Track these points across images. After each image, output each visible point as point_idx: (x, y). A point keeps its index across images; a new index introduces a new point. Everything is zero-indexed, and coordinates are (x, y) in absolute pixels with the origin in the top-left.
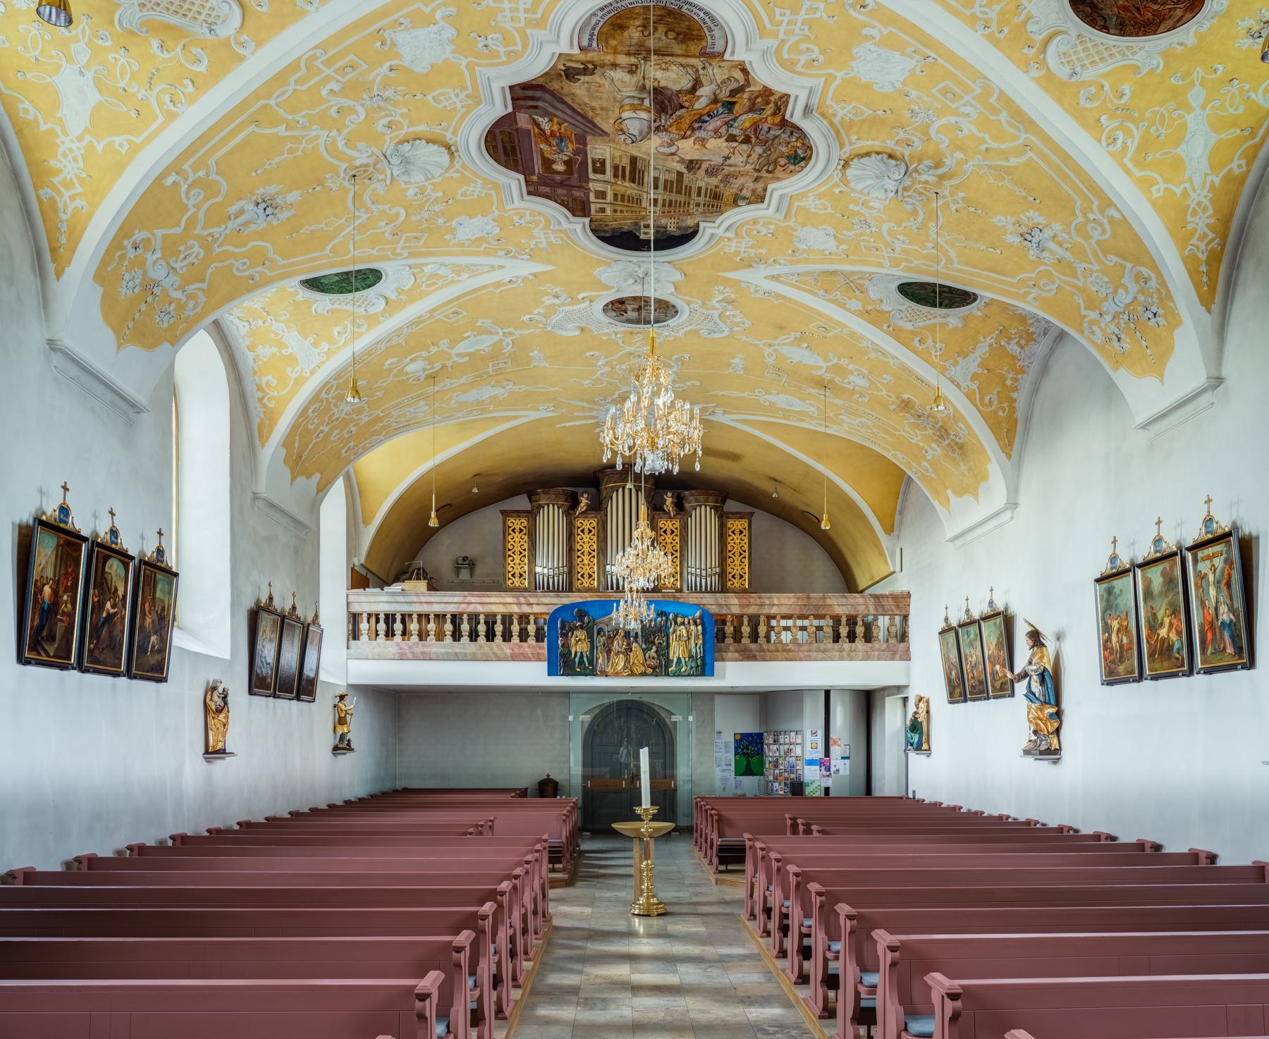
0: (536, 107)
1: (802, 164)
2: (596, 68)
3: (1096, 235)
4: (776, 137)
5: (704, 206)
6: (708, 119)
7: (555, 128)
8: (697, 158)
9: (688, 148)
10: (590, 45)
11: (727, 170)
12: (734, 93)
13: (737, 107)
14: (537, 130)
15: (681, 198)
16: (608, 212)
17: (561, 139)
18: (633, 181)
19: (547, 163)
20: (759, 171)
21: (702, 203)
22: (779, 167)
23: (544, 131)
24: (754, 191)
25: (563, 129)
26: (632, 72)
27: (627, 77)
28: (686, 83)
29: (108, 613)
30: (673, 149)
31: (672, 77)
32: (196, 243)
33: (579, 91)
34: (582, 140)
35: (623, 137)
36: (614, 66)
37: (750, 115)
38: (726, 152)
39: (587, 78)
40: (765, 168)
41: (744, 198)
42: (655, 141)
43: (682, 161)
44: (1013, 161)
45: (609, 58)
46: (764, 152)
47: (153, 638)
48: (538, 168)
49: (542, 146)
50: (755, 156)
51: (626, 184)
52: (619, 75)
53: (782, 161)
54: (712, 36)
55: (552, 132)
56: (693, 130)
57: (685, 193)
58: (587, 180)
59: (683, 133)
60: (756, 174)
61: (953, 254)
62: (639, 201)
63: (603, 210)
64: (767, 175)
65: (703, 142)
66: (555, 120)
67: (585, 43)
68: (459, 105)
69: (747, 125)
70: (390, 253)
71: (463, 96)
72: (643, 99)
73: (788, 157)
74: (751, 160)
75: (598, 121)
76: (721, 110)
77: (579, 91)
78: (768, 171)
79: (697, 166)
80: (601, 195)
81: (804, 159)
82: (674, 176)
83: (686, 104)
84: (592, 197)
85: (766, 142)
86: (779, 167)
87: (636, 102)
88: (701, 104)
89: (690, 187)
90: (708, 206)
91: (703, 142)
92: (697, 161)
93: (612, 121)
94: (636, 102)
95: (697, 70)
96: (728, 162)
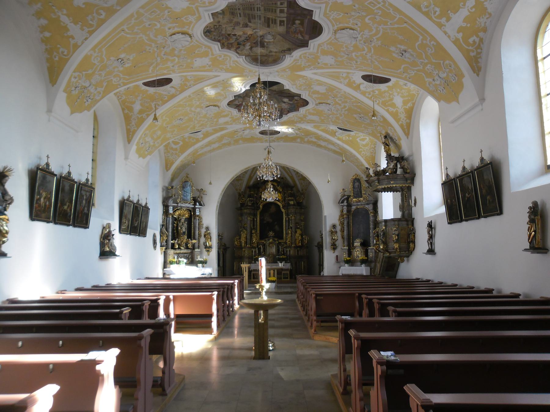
0: (302, 41)
1: (205, 31)
2: (281, 52)
3: (114, 80)
4: (219, 37)
5: (236, 9)
6: (245, 40)
7: (296, 35)
8: (245, 28)
9: (249, 32)
10: (283, 56)
11: (232, 25)
12: (239, 48)
13: (236, 44)
14: (303, 35)
15: (247, 12)
16: (279, 3)
17: (295, 32)
18: (268, 18)
19: (302, 24)
20: (220, 25)
21: (237, 10)
22: (213, 28)
23: (301, 34)
24: (218, 17)
25: (294, 35)
26: (271, 52)
27: (272, 50)
28: (254, 49)
29: (467, 198)
30: (254, 31)
31: (259, 50)
32: (426, 68)
33: (286, 46)
34: (287, 32)
35: (273, 34)
36: (276, 52)
37: (231, 42)
38: (234, 31)
39: (284, 49)
40: (218, 27)
41: (220, 14)
42: (261, 33)
43: (250, 27)
44: (151, 68)
45: (277, 54)
46: (221, 32)
47: (488, 197)
48: (306, 21)
49: (302, 29)
50: (224, 30)
51: (271, 17)
52: (275, 50)
53: (213, 30)
54: (250, 60)
55: (298, 34)
56: (249, 37)
57: (246, 14)
58: (287, 17)
59: (252, 36)
60: (220, 24)
61: (128, 36)
62: (265, 10)
63: (281, 4)
64: (216, 24)
65: (244, 33)
66: (296, 38)
67: (284, 57)
68: (325, 45)
69: (231, 39)
70: (387, 5)
71: (323, 47)
72: (267, 45)
73: (212, 31)
74: (225, 29)
75: (282, 38)
76: (241, 43)
77: (286, 46)
78: (216, 26)
79: (244, 25)
80: (282, 11)
81: (206, 32)
82: (252, 21)
83: (253, 44)
84: (286, 9)
85: (222, 35)
86: (213, 28)
87: (269, 44)
88: (248, 44)
89: (244, 16)
90: (234, 9)
91: (244, 33)
92: (244, 27)
93: (277, 38)
94: (269, 44)
95: (252, 52)
96: (233, 27)
